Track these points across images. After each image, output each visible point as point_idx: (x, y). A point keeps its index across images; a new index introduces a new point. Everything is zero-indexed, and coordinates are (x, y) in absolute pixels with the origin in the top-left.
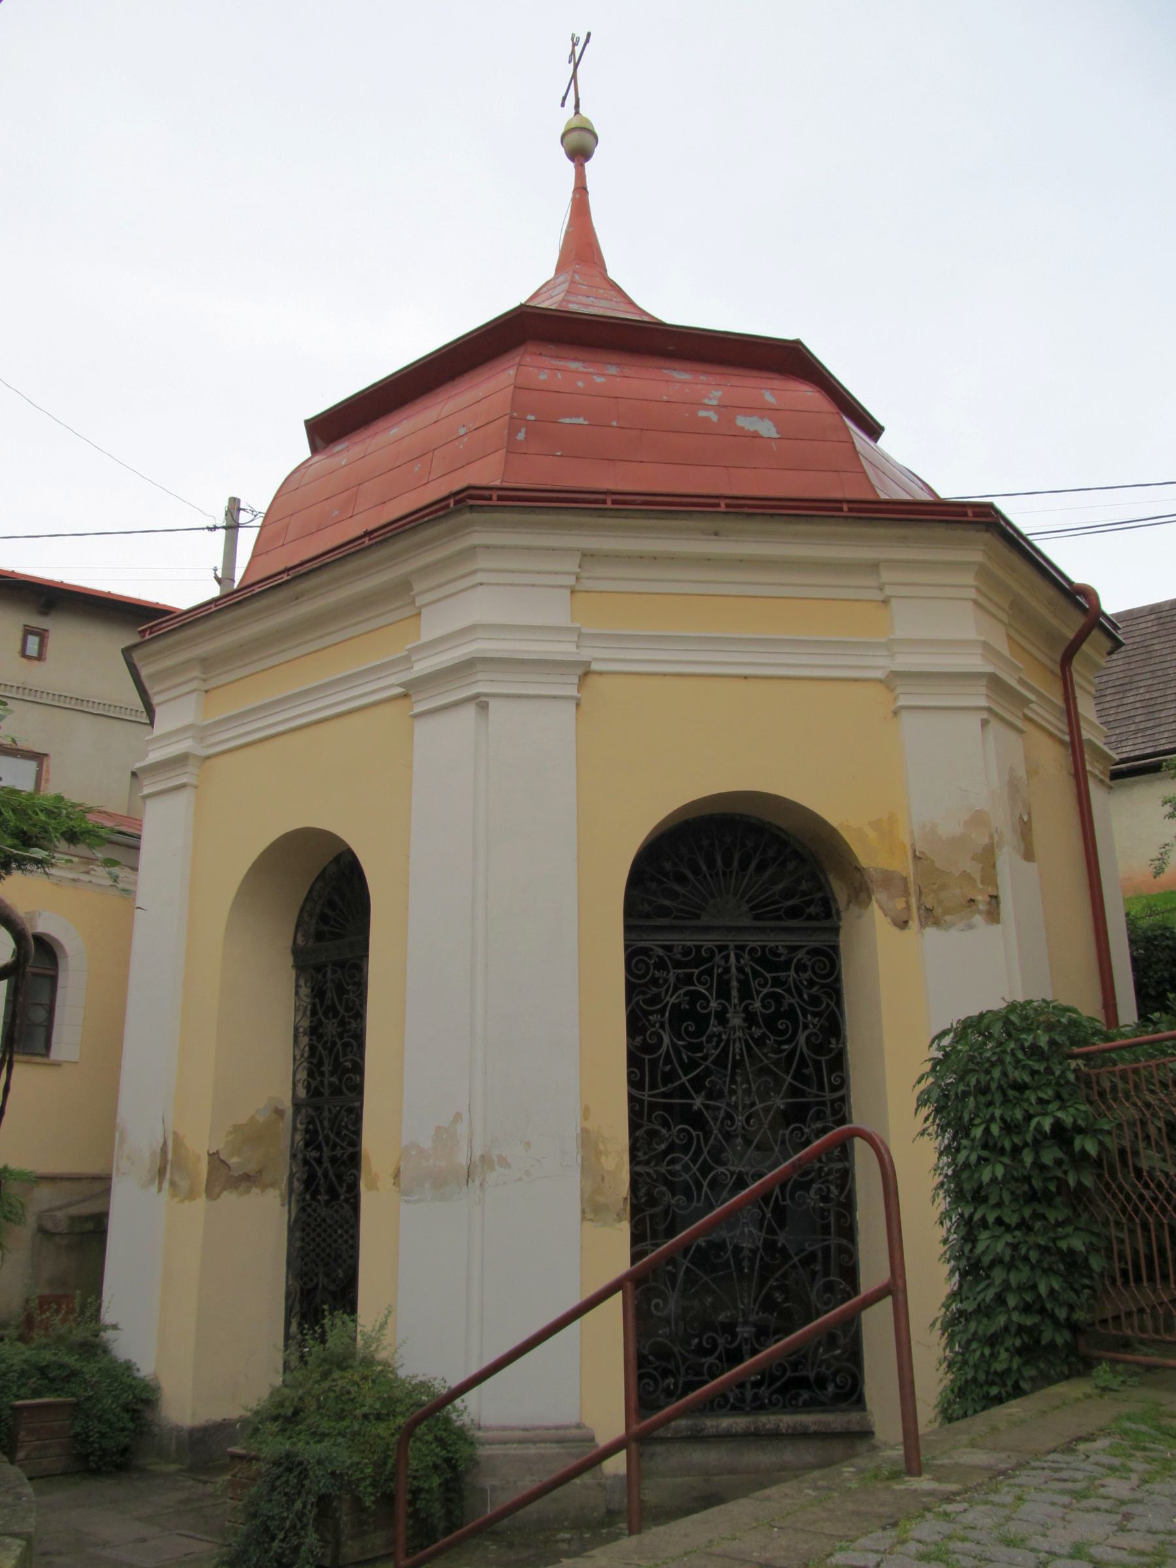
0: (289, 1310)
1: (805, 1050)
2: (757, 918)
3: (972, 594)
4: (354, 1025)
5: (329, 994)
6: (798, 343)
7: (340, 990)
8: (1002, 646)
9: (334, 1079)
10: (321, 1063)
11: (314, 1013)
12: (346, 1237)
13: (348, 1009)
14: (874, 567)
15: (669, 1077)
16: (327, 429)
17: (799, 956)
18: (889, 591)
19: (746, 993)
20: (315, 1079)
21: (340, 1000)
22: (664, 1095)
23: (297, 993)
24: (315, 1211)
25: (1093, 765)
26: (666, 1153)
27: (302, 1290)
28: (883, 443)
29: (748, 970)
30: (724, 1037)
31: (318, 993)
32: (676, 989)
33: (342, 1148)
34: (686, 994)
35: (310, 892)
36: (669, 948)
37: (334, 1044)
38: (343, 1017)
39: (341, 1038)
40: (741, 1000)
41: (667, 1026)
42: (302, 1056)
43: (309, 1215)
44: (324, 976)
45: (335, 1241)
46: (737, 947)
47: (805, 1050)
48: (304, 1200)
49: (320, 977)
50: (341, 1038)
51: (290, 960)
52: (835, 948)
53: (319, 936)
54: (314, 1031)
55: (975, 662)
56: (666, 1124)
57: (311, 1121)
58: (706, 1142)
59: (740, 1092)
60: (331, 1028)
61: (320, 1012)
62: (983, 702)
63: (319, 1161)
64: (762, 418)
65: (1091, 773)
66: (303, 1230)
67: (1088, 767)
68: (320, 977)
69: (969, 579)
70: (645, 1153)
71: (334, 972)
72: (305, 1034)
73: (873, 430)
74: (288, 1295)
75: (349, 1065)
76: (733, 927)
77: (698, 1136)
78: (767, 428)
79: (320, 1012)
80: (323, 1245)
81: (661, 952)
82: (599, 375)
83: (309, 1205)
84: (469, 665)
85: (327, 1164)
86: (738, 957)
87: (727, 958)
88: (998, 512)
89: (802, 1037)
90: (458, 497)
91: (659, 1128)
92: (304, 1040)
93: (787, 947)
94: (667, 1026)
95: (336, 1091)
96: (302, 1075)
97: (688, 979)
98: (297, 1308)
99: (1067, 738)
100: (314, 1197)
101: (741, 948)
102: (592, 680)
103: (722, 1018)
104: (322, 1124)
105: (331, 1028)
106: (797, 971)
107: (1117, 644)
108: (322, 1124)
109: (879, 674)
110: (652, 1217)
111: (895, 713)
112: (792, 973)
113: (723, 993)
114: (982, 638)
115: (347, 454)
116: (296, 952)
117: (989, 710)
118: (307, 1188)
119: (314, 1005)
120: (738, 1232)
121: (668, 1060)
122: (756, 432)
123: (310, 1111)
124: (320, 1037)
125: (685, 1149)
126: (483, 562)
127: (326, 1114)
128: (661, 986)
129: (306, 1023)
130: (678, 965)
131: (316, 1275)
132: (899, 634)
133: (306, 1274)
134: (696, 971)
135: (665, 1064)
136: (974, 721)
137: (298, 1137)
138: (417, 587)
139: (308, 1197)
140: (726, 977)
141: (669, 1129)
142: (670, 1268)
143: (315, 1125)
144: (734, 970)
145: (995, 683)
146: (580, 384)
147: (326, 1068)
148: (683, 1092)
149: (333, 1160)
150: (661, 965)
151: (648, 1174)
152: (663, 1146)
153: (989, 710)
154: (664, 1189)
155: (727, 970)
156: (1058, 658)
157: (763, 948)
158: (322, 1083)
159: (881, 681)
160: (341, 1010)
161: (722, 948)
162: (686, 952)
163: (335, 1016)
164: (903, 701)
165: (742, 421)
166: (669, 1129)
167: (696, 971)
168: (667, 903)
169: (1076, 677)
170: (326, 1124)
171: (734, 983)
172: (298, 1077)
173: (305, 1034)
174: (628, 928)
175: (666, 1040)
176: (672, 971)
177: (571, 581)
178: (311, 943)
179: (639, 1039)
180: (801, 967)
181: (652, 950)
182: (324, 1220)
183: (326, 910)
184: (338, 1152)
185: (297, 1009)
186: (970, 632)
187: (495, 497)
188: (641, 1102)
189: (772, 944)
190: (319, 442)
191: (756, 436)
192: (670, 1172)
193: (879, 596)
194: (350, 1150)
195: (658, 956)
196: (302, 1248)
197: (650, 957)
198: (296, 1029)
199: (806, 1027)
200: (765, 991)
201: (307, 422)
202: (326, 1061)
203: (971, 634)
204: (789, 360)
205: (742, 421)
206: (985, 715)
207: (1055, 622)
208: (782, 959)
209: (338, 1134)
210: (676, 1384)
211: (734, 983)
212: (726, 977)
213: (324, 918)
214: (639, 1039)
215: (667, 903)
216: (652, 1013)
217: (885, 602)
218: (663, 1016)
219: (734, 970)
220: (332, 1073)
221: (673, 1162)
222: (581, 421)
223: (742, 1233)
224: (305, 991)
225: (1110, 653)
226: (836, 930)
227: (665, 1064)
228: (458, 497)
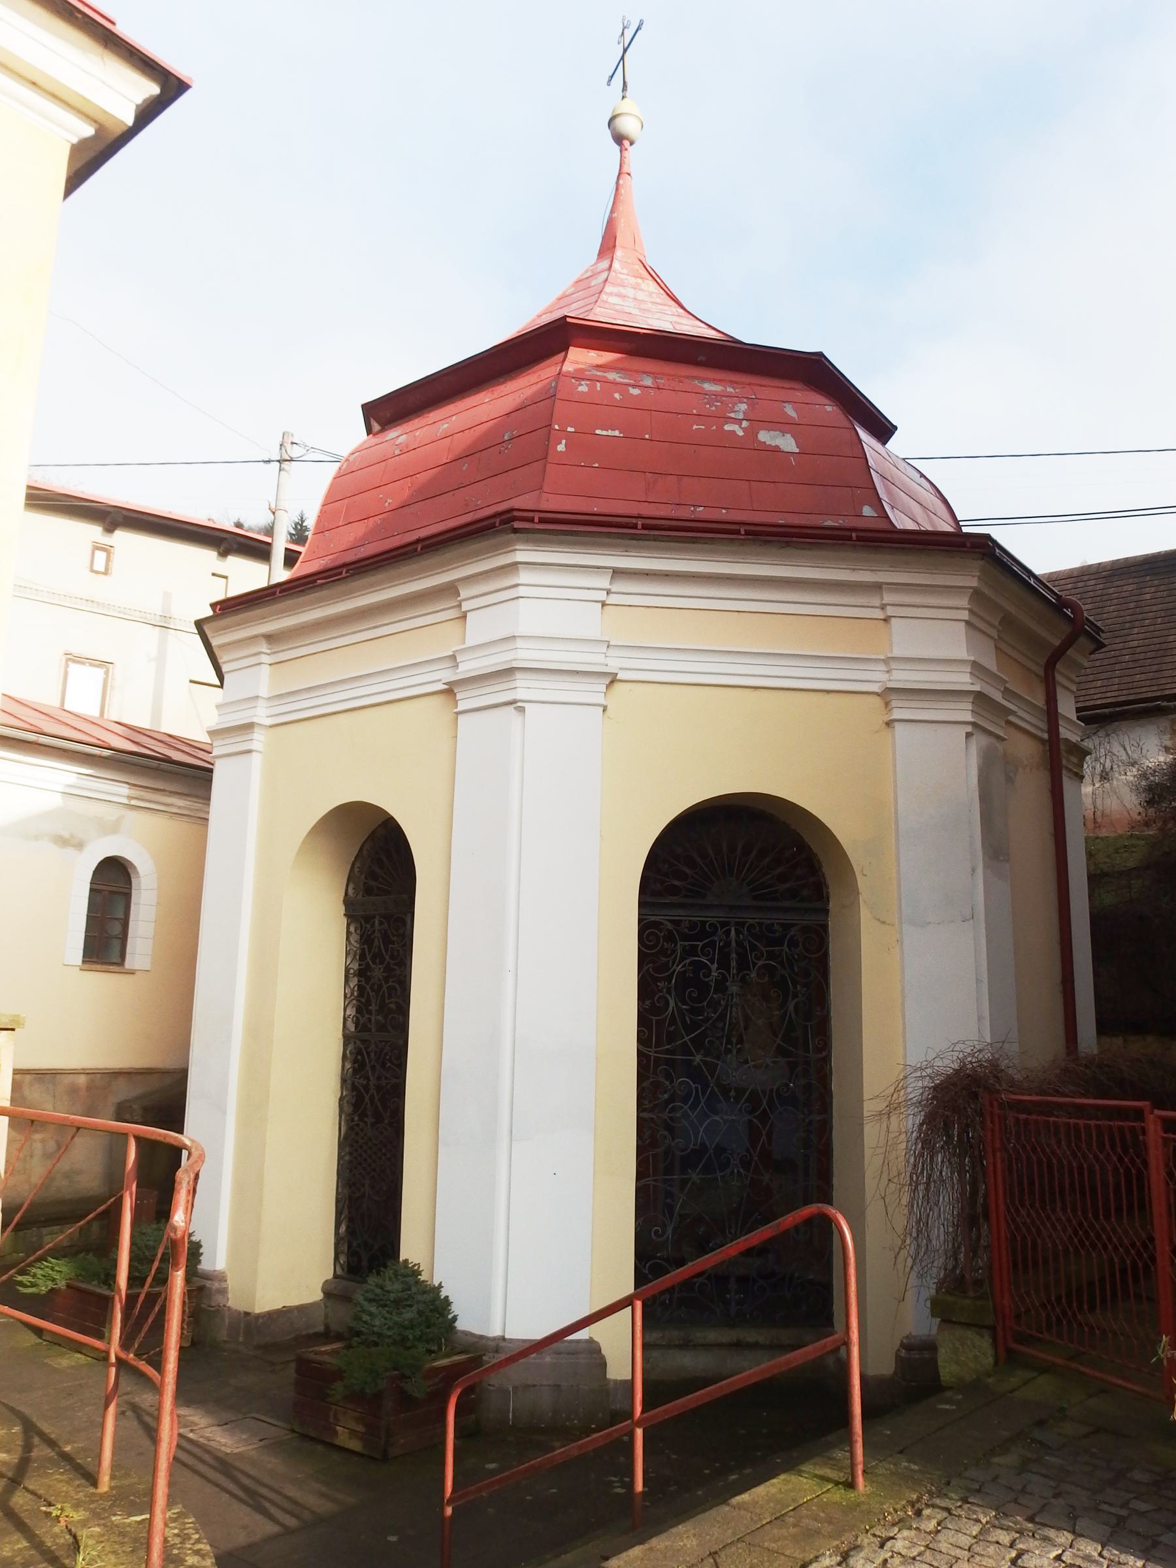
0: (339, 1213)
1: (793, 1015)
2: (755, 898)
3: (965, 615)
4: (398, 972)
5: (376, 943)
6: (821, 354)
7: (387, 940)
8: (991, 664)
9: (379, 1018)
10: (368, 1002)
11: (362, 957)
12: (389, 1156)
13: (392, 957)
14: (877, 587)
15: (671, 1038)
16: (384, 413)
17: (792, 933)
18: (890, 611)
19: (743, 965)
20: (363, 1016)
21: (387, 951)
22: (667, 1052)
23: (347, 939)
24: (362, 1130)
25: (1068, 760)
26: (668, 1102)
27: (350, 1197)
28: (895, 444)
29: (746, 944)
30: (722, 1002)
31: (366, 939)
32: (682, 959)
33: (386, 1078)
34: (691, 963)
35: (361, 850)
36: (676, 923)
37: (380, 986)
38: (389, 963)
39: (387, 982)
40: (739, 969)
41: (673, 993)
42: (352, 994)
43: (357, 1134)
44: (373, 925)
45: (380, 1158)
46: (737, 924)
47: (793, 1015)
48: (353, 1120)
49: (368, 926)
50: (387, 982)
51: (342, 909)
52: (825, 927)
53: (368, 891)
54: (362, 973)
55: (963, 679)
56: (668, 1077)
57: (359, 1052)
58: (704, 1093)
59: (734, 1051)
60: (377, 972)
61: (368, 957)
62: (969, 717)
63: (366, 1088)
64: (784, 432)
65: (1067, 768)
66: (351, 1146)
67: (1064, 762)
68: (368, 926)
69: (964, 602)
70: (650, 1102)
71: (381, 923)
72: (355, 975)
73: (883, 430)
74: (337, 1201)
75: (393, 1006)
76: (735, 907)
77: (697, 1089)
78: (788, 444)
79: (368, 957)
80: (369, 1160)
81: (670, 926)
82: (634, 386)
83: (358, 1125)
84: (508, 672)
85: (373, 1091)
86: (738, 932)
87: (728, 933)
88: (995, 542)
89: (791, 1006)
90: (504, 517)
91: (662, 1080)
92: (354, 982)
93: (782, 925)
94: (673, 993)
95: (382, 1028)
96: (351, 1011)
97: (692, 951)
98: (346, 1212)
99: (1046, 736)
100: (361, 1119)
101: (743, 924)
102: (618, 687)
103: (721, 986)
104: (369, 1055)
105: (377, 972)
106: (789, 947)
107: (1100, 645)
108: (369, 1055)
109: (875, 688)
110: (655, 1156)
111: (889, 724)
112: (785, 947)
113: (724, 964)
114: (972, 658)
115: (397, 435)
116: (348, 902)
117: (974, 724)
118: (355, 1112)
119: (363, 950)
120: (728, 1171)
121: (673, 1020)
122: (777, 446)
123: (358, 1042)
124: (368, 979)
125: (685, 1100)
126: (524, 576)
127: (373, 1047)
128: (669, 956)
129: (355, 966)
130: (685, 938)
131: (363, 1185)
132: (897, 652)
133: (354, 1184)
134: (701, 944)
135: (670, 1025)
136: (963, 731)
137: (348, 1065)
138: (464, 593)
139: (356, 1118)
140: (726, 950)
141: (672, 1082)
142: (669, 1201)
143: (362, 1055)
144: (734, 944)
145: (980, 699)
146: (617, 396)
147: (373, 1008)
148: (684, 1182)
149: (379, 1088)
150: (670, 937)
151: (652, 1119)
152: (666, 1096)
153: (974, 724)
154: (666, 1133)
155: (728, 944)
156: (1043, 661)
157: (761, 924)
158: (370, 1020)
159: (877, 694)
160: (387, 958)
161: (724, 924)
162: (693, 926)
163: (381, 963)
164: (896, 714)
165: (764, 436)
166: (672, 1082)
167: (701, 944)
168: (676, 883)
169: (1058, 678)
170: (372, 1055)
171: (734, 955)
172: (348, 1013)
173: (355, 975)
174: (642, 904)
175: (672, 1003)
176: (679, 943)
177: (602, 596)
178: (360, 897)
179: (648, 1002)
180: (793, 943)
181: (661, 923)
182: (370, 1139)
183: (377, 870)
184: (383, 1082)
185: (347, 954)
186: (962, 653)
187: (536, 520)
188: (648, 1057)
189: (769, 922)
190: (376, 427)
191: (776, 450)
192: (671, 1118)
193: (879, 614)
194: (394, 1081)
195: (668, 930)
196: (350, 1162)
197: (660, 931)
198: (347, 970)
199: (795, 996)
200: (760, 963)
201: (363, 406)
202: (373, 1001)
203: (962, 653)
204: (814, 372)
205: (764, 436)
206: (969, 729)
207: (1043, 633)
208: (777, 935)
209: (383, 1065)
210: (670, 1301)
211: (734, 955)
212: (726, 950)
213: (372, 875)
214: (648, 1002)
215: (676, 883)
216: (660, 980)
217: (886, 620)
218: (670, 983)
219: (734, 944)
220: (379, 1012)
221: (673, 1110)
222: (617, 433)
223: (732, 1173)
224: (355, 938)
225: (1092, 653)
226: (826, 912)
227: (670, 1025)
228: (504, 517)
